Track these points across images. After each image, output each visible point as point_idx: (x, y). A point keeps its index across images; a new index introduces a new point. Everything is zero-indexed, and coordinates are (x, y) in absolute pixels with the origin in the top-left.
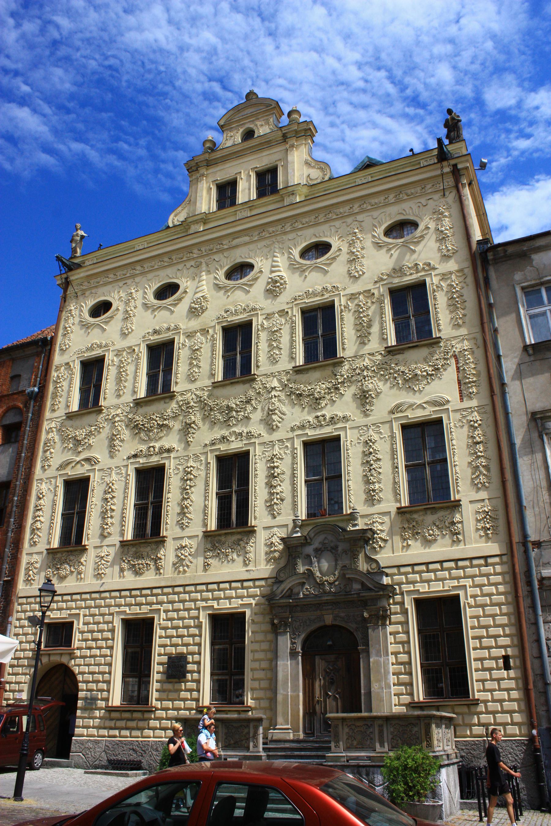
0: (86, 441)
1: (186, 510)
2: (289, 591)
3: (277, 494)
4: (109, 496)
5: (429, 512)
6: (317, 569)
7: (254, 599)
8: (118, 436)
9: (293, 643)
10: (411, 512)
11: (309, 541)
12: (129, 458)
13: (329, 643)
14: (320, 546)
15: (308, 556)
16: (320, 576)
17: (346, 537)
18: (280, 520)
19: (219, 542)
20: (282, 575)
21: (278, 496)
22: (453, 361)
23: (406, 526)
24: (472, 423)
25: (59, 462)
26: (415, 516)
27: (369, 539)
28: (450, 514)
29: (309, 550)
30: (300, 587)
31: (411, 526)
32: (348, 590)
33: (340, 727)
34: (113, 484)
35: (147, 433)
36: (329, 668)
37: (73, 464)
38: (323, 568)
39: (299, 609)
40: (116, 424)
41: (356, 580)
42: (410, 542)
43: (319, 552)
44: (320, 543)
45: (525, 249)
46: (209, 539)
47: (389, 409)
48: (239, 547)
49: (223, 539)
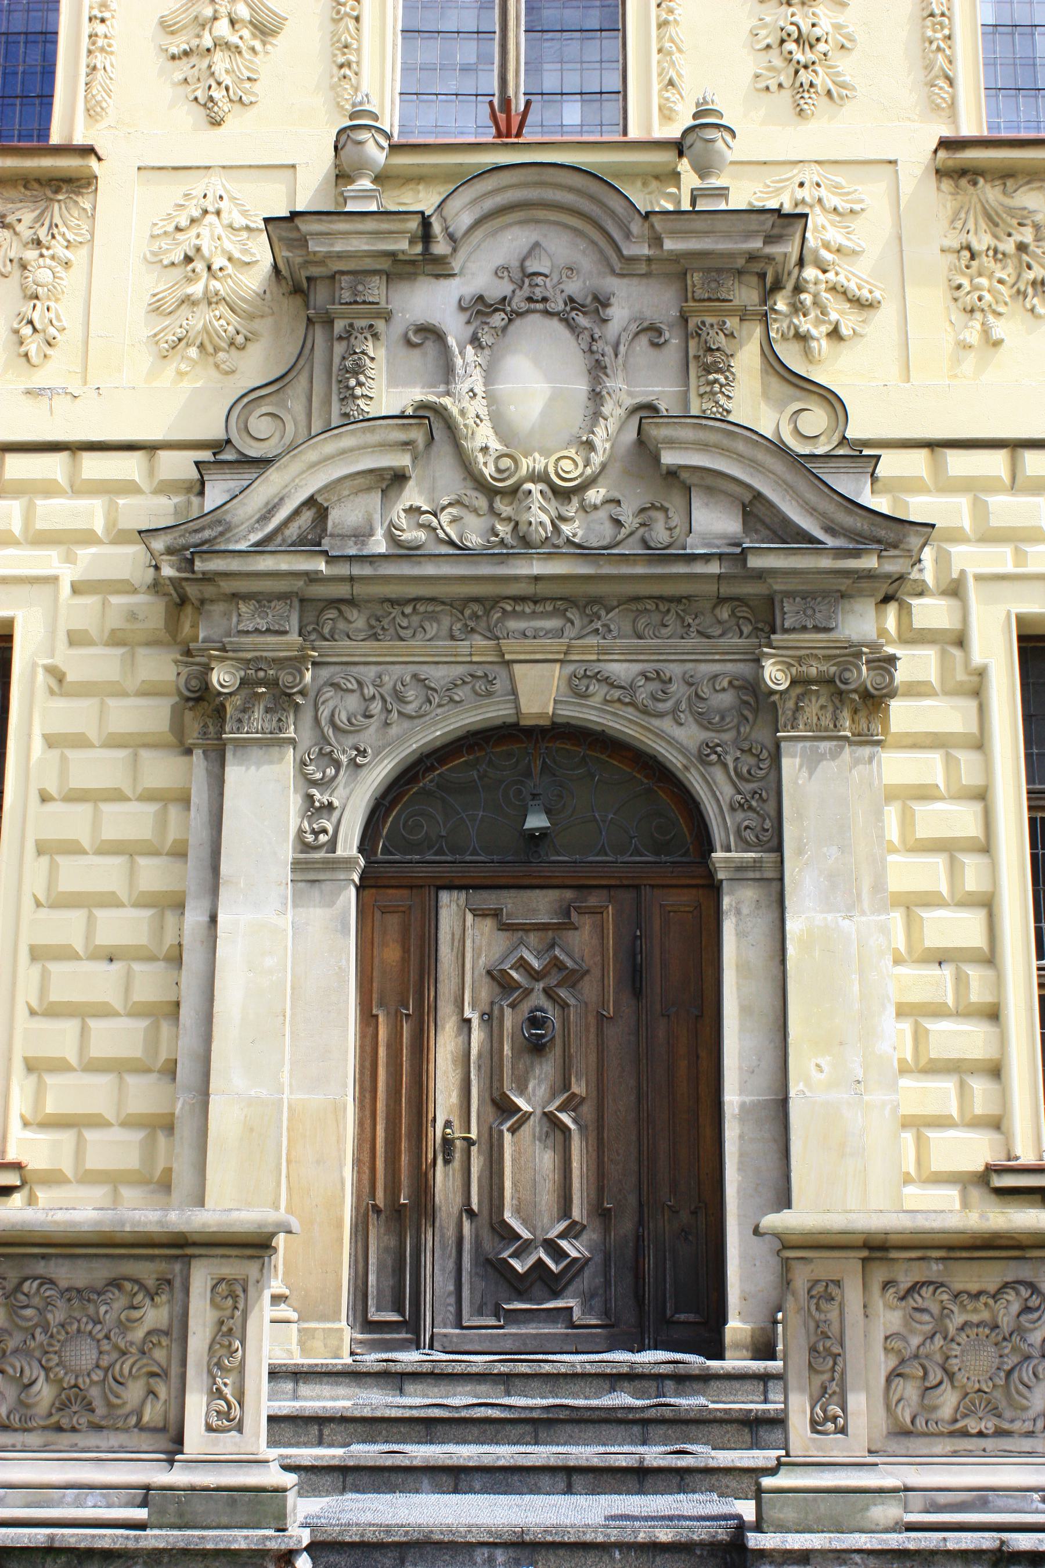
2: (308, 515)
6: (478, 406)
7: (70, 559)
9: (315, 809)
10: (1006, 175)
11: (441, 247)
13: (536, 821)
14: (504, 288)
15: (430, 334)
16: (495, 445)
17: (669, 245)
20: (260, 426)
23: (982, 241)
27: (777, 286)
29: (435, 302)
30: (376, 497)
31: (1008, 246)
32: (660, 534)
33: (853, 1295)
36: (522, 964)
38: (528, 398)
39: (358, 620)
41: (713, 483)
42: (1000, 329)
44: (501, 271)
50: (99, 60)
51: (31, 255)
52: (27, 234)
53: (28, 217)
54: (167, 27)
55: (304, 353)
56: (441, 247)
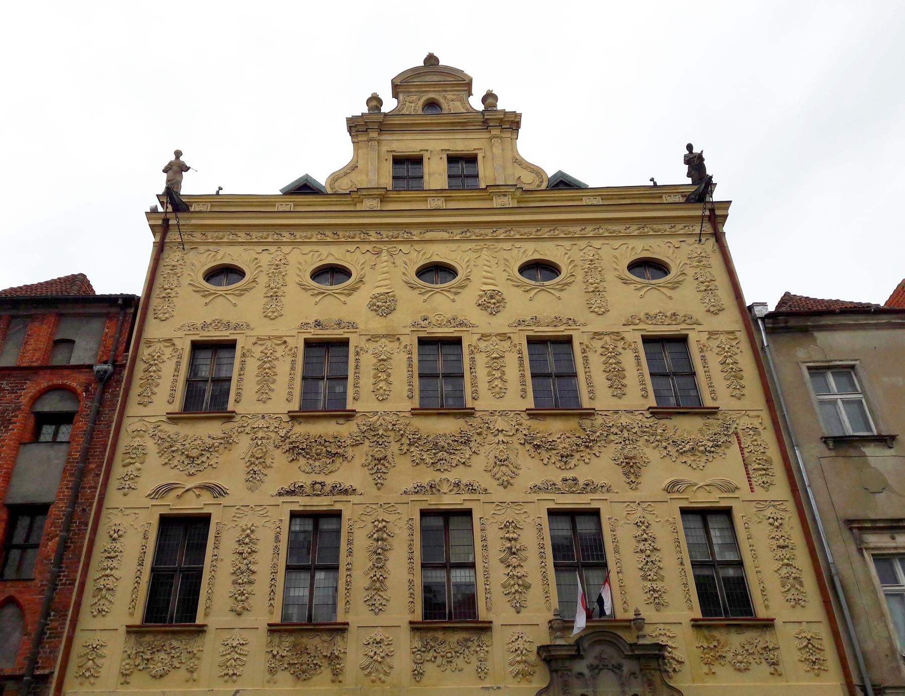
0: (204, 459)
1: (378, 585)
3: (519, 578)
4: (246, 549)
5: (733, 630)
8: (262, 460)
12: (280, 494)
14: (596, 662)
15: (581, 674)
17: (636, 653)
18: (526, 616)
19: (435, 639)
21: (520, 582)
22: (734, 439)
24: (771, 520)
25: (154, 487)
26: (716, 634)
28: (760, 636)
34: (252, 531)
35: (311, 462)
37: (180, 492)
40: (259, 442)
43: (597, 671)
44: (596, 658)
45: (809, 324)
46: (418, 634)
47: (663, 486)
48: (467, 651)
49: (440, 635)
50: (488, 595)
51: (478, 649)
52: (476, 644)
53: (476, 638)
54: (504, 586)
55: (552, 680)
56: (582, 653)
